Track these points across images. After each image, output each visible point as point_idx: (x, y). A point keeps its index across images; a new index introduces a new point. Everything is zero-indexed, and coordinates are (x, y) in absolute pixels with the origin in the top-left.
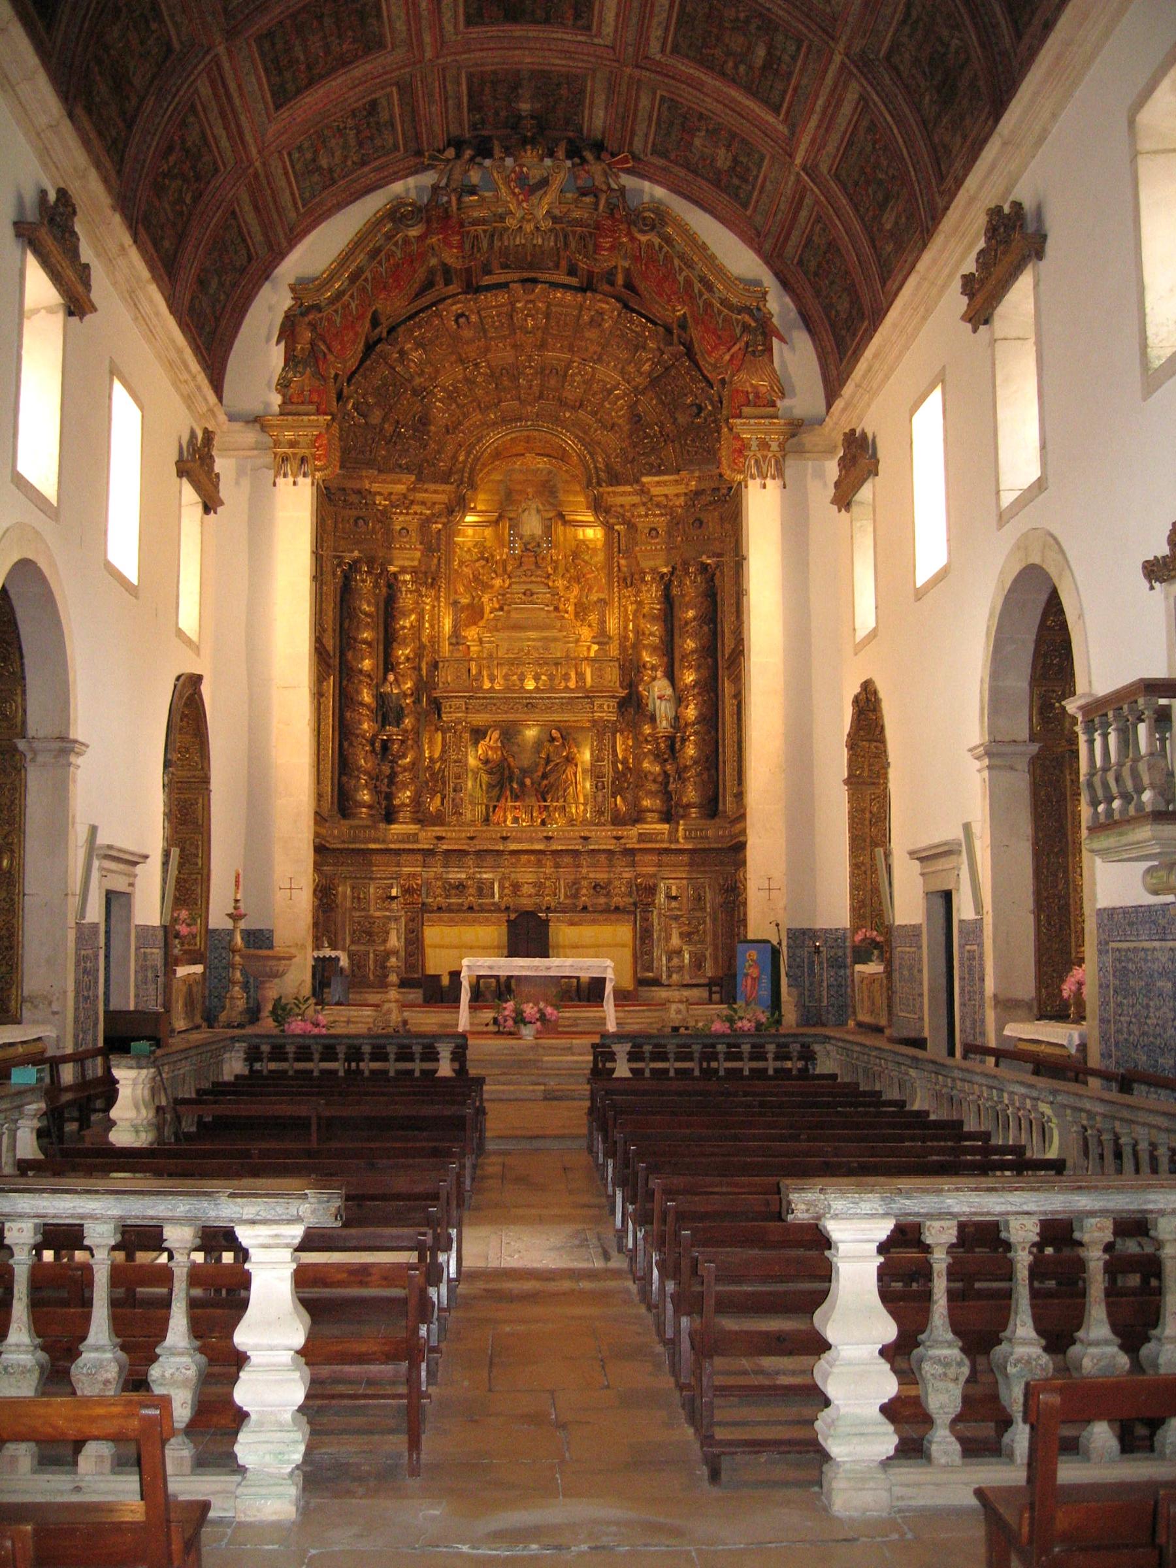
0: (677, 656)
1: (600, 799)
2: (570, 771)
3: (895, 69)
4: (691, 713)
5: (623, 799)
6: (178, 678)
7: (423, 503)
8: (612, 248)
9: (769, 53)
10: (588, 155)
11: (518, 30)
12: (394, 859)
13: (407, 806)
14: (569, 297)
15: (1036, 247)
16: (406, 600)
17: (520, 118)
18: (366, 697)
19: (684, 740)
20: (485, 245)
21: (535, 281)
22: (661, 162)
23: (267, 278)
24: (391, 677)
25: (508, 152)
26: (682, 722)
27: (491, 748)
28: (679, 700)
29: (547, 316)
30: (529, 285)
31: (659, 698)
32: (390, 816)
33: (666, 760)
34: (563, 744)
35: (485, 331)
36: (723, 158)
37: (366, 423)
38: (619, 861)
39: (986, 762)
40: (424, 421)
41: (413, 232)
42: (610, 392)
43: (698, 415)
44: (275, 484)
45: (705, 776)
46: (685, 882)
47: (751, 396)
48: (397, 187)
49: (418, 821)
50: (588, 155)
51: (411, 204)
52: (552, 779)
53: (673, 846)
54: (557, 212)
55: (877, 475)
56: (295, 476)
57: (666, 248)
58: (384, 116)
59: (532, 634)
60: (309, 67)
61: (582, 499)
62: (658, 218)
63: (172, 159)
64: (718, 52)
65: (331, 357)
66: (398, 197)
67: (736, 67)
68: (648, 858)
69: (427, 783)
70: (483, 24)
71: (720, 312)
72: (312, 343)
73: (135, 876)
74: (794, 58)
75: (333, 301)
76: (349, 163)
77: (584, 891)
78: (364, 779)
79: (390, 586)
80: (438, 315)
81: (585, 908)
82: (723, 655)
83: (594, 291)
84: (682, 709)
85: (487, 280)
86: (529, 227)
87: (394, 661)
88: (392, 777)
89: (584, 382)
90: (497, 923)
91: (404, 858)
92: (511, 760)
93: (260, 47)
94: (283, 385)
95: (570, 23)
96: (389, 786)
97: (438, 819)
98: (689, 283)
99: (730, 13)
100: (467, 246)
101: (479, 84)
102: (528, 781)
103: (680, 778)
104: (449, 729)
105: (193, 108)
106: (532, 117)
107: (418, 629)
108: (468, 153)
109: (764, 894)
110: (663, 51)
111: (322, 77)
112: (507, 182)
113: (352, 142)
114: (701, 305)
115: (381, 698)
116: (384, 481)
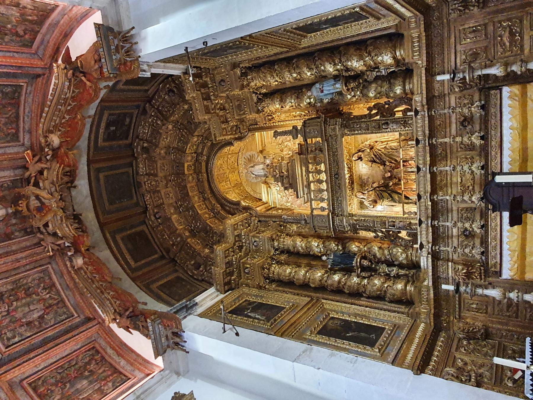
2: (379, 147)
4: (330, 69)
10: (27, 174)
13: (407, 256)
19: (347, 70)
26: (336, 73)
27: (368, 198)
28: (322, 78)
33: (366, 80)
37: (203, 264)
43: (173, 92)
44: (188, 352)
52: (385, 159)
71: (73, 92)
79: (282, 252)
82: (287, 52)
92: (375, 185)
97: (414, 236)
98: (68, 112)
103: (376, 68)
106: (11, 207)
114: (74, 104)
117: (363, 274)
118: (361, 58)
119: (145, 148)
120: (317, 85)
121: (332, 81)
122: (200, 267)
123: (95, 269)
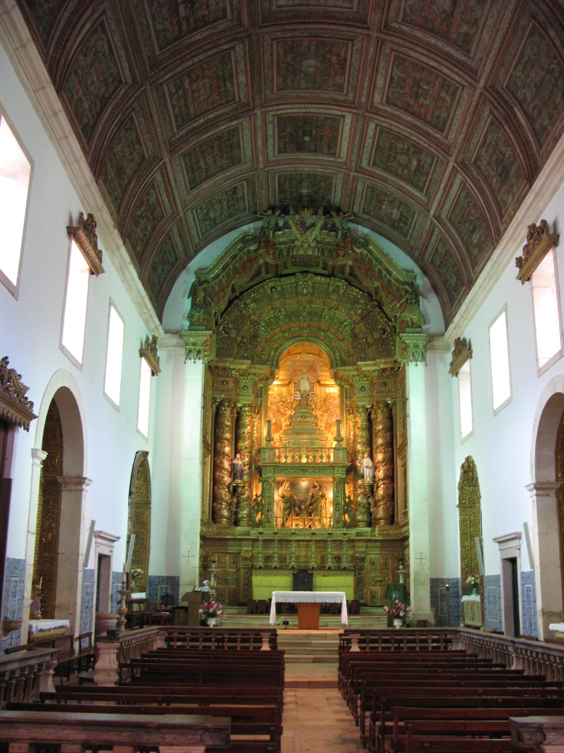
0: (374, 446)
1: (337, 515)
2: (323, 502)
3: (479, 168)
4: (380, 474)
5: (349, 516)
6: (137, 453)
7: (254, 374)
8: (344, 256)
9: (418, 164)
10: (334, 214)
11: (302, 156)
12: (238, 543)
14: (323, 279)
15: (554, 241)
16: (247, 420)
17: (302, 197)
18: (226, 464)
19: (378, 487)
20: (285, 254)
21: (307, 272)
22: (366, 217)
23: (184, 268)
24: (238, 456)
25: (297, 213)
26: (377, 479)
28: (375, 468)
29: (313, 288)
30: (305, 274)
31: (366, 467)
32: (236, 523)
33: (369, 497)
34: (320, 490)
35: (284, 295)
36: (396, 214)
38: (345, 545)
39: (535, 492)
40: (255, 336)
41: (252, 248)
42: (342, 323)
43: (384, 333)
45: (388, 505)
46: (379, 556)
47: (410, 324)
48: (245, 228)
49: (250, 526)
50: (334, 214)
51: (252, 235)
52: (315, 505)
53: (373, 538)
54: (319, 239)
55: (471, 357)
56: (195, 359)
57: (369, 255)
58: (240, 194)
59: (305, 436)
60: (206, 170)
61: (328, 374)
62: (366, 243)
63: (143, 209)
64: (394, 164)
65: (213, 304)
66: (245, 232)
67: (403, 171)
68: (361, 544)
69: (254, 507)
70: (286, 153)
71: (395, 285)
72: (204, 298)
73: (113, 547)
74: (430, 166)
75: (214, 279)
76: (223, 216)
77: (329, 560)
78: (224, 504)
79: (238, 413)
80: (263, 287)
81: (329, 568)
83: (335, 277)
84: (377, 472)
85: (285, 272)
86: (305, 246)
87: (239, 448)
88: (238, 504)
89: (330, 319)
90: (288, 575)
91: (243, 543)
93: (184, 160)
94: (190, 317)
95: (326, 152)
96: (236, 508)
97: (260, 524)
98: (380, 271)
99: (400, 146)
100: (277, 254)
101: (284, 180)
102: (303, 507)
104: (265, 481)
105: (153, 186)
107: (251, 433)
108: (278, 213)
109: (418, 561)
110: (369, 164)
111: (212, 176)
112: (296, 225)
113: (225, 206)
115: (233, 466)
116: (236, 364)
117: (231, 488)
118: (383, 498)
119: (339, 290)
120: (370, 464)
121: (371, 475)
122: (226, 333)
123: (244, 263)
